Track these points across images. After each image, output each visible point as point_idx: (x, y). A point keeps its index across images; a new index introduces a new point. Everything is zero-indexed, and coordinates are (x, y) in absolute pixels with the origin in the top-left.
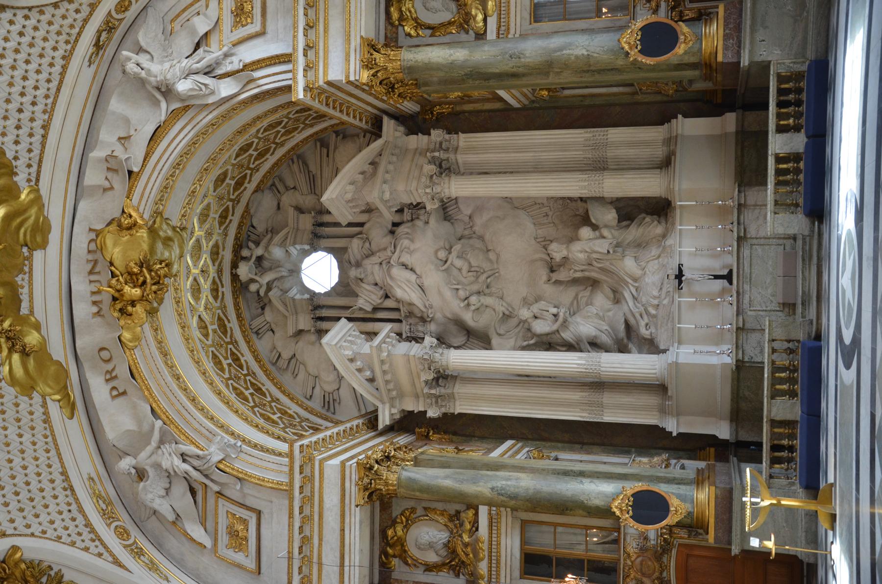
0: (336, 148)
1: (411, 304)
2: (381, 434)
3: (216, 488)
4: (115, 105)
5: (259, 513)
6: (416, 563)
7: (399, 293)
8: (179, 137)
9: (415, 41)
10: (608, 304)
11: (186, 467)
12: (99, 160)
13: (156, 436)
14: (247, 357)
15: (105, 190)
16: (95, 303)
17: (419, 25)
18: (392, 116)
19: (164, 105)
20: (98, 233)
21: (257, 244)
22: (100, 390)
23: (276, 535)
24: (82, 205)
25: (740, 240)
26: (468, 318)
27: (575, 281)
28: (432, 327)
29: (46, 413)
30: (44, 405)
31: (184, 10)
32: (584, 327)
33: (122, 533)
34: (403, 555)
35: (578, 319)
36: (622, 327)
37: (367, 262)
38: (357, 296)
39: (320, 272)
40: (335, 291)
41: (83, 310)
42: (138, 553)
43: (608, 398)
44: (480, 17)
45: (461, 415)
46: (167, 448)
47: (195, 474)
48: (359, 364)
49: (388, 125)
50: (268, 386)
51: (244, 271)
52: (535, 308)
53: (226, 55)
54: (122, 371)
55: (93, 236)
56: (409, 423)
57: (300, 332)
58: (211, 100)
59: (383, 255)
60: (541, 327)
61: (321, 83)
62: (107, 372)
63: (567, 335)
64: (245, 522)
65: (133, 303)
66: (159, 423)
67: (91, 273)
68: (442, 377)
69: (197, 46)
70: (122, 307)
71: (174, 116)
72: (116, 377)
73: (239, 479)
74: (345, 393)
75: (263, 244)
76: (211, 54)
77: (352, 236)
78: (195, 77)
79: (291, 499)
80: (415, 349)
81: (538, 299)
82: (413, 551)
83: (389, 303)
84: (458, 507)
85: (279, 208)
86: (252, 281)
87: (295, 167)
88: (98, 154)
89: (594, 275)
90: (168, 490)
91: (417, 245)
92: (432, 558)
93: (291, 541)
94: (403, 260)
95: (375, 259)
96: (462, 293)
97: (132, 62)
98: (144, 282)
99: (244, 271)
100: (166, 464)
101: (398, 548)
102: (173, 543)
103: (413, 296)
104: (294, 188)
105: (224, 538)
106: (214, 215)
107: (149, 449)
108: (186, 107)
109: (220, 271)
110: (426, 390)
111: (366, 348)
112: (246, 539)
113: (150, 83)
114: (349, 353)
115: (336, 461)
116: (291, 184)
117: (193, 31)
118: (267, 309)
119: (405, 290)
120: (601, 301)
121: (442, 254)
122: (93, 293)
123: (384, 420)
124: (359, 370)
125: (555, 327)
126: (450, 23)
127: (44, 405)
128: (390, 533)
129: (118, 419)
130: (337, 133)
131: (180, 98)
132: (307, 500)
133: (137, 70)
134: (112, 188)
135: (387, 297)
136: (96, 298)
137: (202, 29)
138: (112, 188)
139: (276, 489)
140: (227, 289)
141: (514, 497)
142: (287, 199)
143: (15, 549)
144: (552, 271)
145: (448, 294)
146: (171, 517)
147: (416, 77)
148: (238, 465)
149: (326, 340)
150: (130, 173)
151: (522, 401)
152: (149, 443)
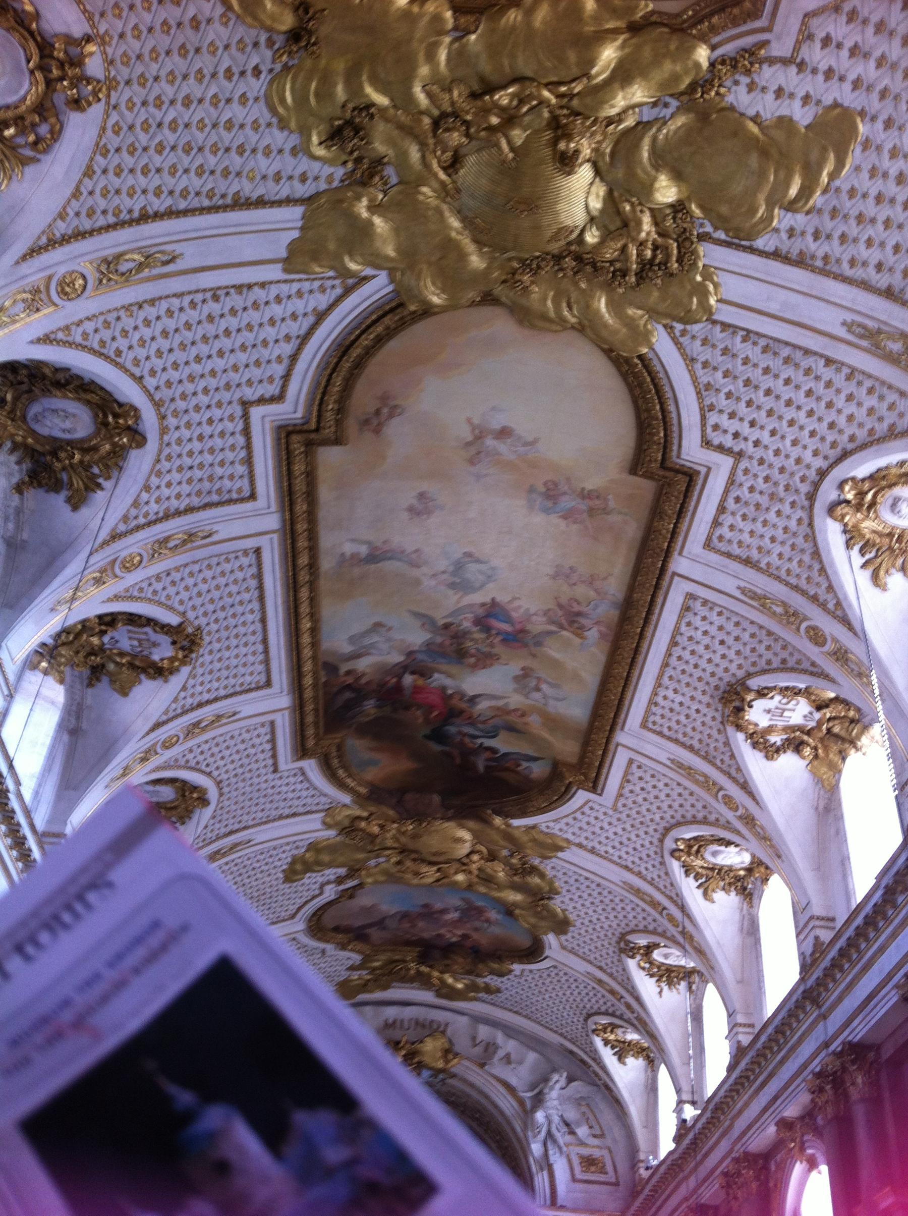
4: (532, 1057)
8: (506, 1104)
12: (495, 1038)
16: (394, 1022)
19: (529, 1094)
20: (443, 1032)
31: (595, 1116)
41: (391, 1012)
53: (560, 1148)
58: (530, 1134)
69: (567, 1124)
71: (521, 1102)
76: (562, 1138)
88: (500, 1038)
97: (559, 1079)
108: (527, 1113)
113: (545, 1086)
117: (579, 1125)
133: (554, 1080)
136: (398, 1024)
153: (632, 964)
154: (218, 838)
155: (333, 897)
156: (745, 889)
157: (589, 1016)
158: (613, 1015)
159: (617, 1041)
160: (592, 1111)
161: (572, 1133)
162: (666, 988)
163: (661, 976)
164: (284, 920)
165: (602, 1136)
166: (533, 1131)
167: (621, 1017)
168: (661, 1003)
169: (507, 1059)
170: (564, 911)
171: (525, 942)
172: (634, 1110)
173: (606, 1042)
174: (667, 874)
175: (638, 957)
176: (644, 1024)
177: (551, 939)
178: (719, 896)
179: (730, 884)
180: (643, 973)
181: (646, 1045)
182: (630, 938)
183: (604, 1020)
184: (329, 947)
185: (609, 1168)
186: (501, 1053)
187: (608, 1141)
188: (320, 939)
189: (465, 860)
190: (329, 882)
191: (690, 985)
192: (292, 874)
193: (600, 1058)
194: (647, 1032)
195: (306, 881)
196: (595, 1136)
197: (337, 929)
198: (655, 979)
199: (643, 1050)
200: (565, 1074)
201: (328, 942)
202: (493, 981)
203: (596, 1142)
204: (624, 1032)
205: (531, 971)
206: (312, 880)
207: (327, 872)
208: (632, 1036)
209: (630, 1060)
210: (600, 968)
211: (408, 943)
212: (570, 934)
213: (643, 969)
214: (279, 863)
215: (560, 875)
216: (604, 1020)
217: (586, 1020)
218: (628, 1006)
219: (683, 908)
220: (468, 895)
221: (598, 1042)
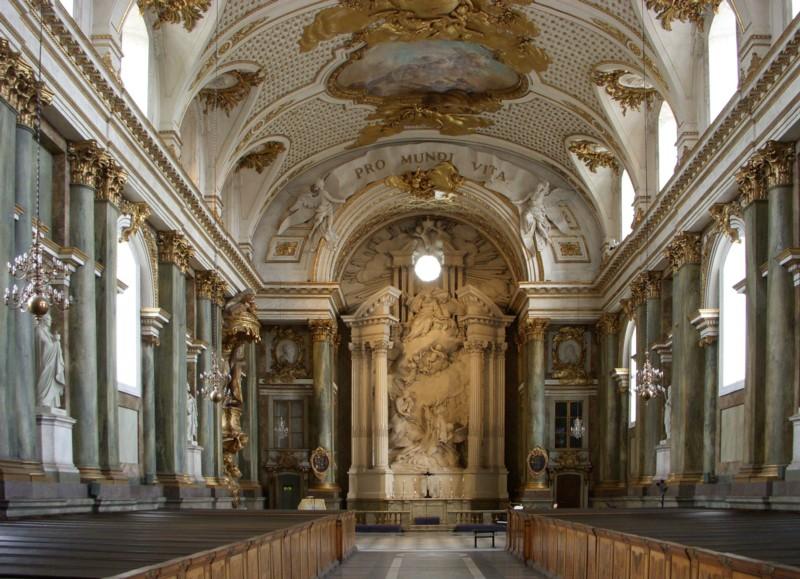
0: (500, 279)
1: (410, 330)
2: (336, 315)
3: (310, 236)
4: (521, 173)
5: (298, 262)
6: (275, 345)
7: (417, 323)
8: (503, 211)
9: (550, 343)
10: (413, 437)
11: (321, 219)
13: (338, 201)
14: (376, 228)
15: (474, 164)
16: (410, 157)
17: (559, 343)
18: (517, 319)
19: (521, 202)
20: (449, 162)
21: (445, 230)
22: (359, 163)
23: (289, 274)
24: (466, 148)
25: (446, 501)
26: (404, 363)
27: (424, 420)
28: (398, 341)
29: (349, 140)
30: (353, 139)
31: (572, 213)
32: (401, 426)
33: (282, 184)
34: (278, 338)
35: (405, 422)
36: (401, 445)
37: (434, 303)
38: (415, 295)
39: (428, 267)
40: (417, 281)
41: (406, 150)
42: (272, 195)
43: (364, 440)
44: (560, 375)
45: (350, 362)
46: (331, 207)
47: (317, 224)
48: (377, 305)
49: (511, 319)
50: (359, 242)
51: (428, 224)
52: (410, 399)
53: (546, 240)
54: (372, 177)
55: (448, 159)
56: (344, 331)
57: (391, 257)
58: (522, 232)
59: (438, 313)
60: (400, 402)
61: (528, 296)
62: (371, 166)
63: (395, 417)
64: (294, 251)
65: (410, 183)
66: (344, 201)
67: (427, 155)
68: (370, 351)
69: (550, 222)
70: (407, 177)
71: (514, 209)
72: (368, 172)
73: (317, 250)
74: (356, 287)
75: (445, 234)
77: (449, 291)
78: (534, 223)
79: (309, 282)
80: (386, 338)
81: (414, 400)
82: (282, 343)
83: (411, 315)
84: (308, 367)
85: (466, 241)
86: (423, 229)
87: (491, 253)
88: (495, 161)
89: (429, 430)
90: (307, 207)
91: (444, 333)
92: (279, 354)
93: (288, 284)
94: (435, 325)
95: (436, 307)
96: (417, 358)
97: (543, 187)
98: (423, 189)
99: (428, 224)
100: (322, 208)
101: (281, 335)
102: (277, 210)
103: (415, 331)
104: (479, 252)
105: (282, 241)
106: (462, 211)
107: (330, 197)
109: (428, 210)
110: (364, 343)
111: (386, 310)
112: (283, 254)
114: (383, 299)
115: (329, 307)
116: (483, 248)
118: (404, 235)
119: (419, 325)
120: (415, 433)
121: (438, 347)
122: (415, 156)
123: (346, 319)
124: (373, 305)
125: (400, 411)
126: (558, 360)
127: (353, 139)
128: (290, 331)
129: (344, 175)
130: (510, 280)
131: (524, 214)
132: (310, 292)
133: (539, 190)
134: (475, 169)
135: (414, 314)
137: (560, 226)
138: (475, 169)
139: (312, 272)
140: (417, 213)
141: (320, 401)
142: (471, 247)
143: (285, 149)
144: (430, 407)
145: (416, 352)
146: (292, 209)
147: (530, 344)
148: (324, 248)
149: (392, 288)
150: (484, 182)
151: (359, 395)
152: (334, 197)
153: (601, 90)
154: (238, 20)
155: (345, 59)
156: (697, 15)
157: (566, 136)
158: (586, 134)
159: (589, 154)
160: (570, 211)
161: (555, 227)
162: (628, 108)
163: (625, 99)
164: (308, 84)
165: (578, 228)
166: (524, 229)
167: (592, 135)
168: (623, 120)
169: (502, 176)
170: (542, 50)
171: (510, 81)
172: (603, 208)
173: (580, 156)
174: (631, 8)
175: (606, 84)
176: (609, 138)
177: (533, 75)
178: (676, 24)
179: (685, 12)
180: (610, 97)
181: (612, 155)
182: (599, 68)
183: (579, 139)
184: (348, 103)
185: (583, 250)
186: (497, 173)
187: (583, 231)
188: (340, 97)
189: (454, 14)
190: (339, 47)
191: (648, 103)
192: (305, 44)
193: (576, 169)
194: (613, 145)
195: (320, 48)
196: (572, 228)
197: (352, 87)
198: (619, 102)
199: (610, 159)
200: (548, 184)
201: (347, 98)
202: (486, 115)
203: (573, 232)
204: (595, 147)
205: (517, 105)
206: (324, 47)
207: (336, 38)
208: (601, 149)
209: (600, 169)
210: (575, 96)
211: (414, 92)
212: (549, 70)
213: (610, 93)
214: (293, 36)
215: (538, 18)
216: (579, 139)
217: (563, 141)
218: (598, 126)
219: (644, 38)
220: (460, 44)
221: (574, 157)
